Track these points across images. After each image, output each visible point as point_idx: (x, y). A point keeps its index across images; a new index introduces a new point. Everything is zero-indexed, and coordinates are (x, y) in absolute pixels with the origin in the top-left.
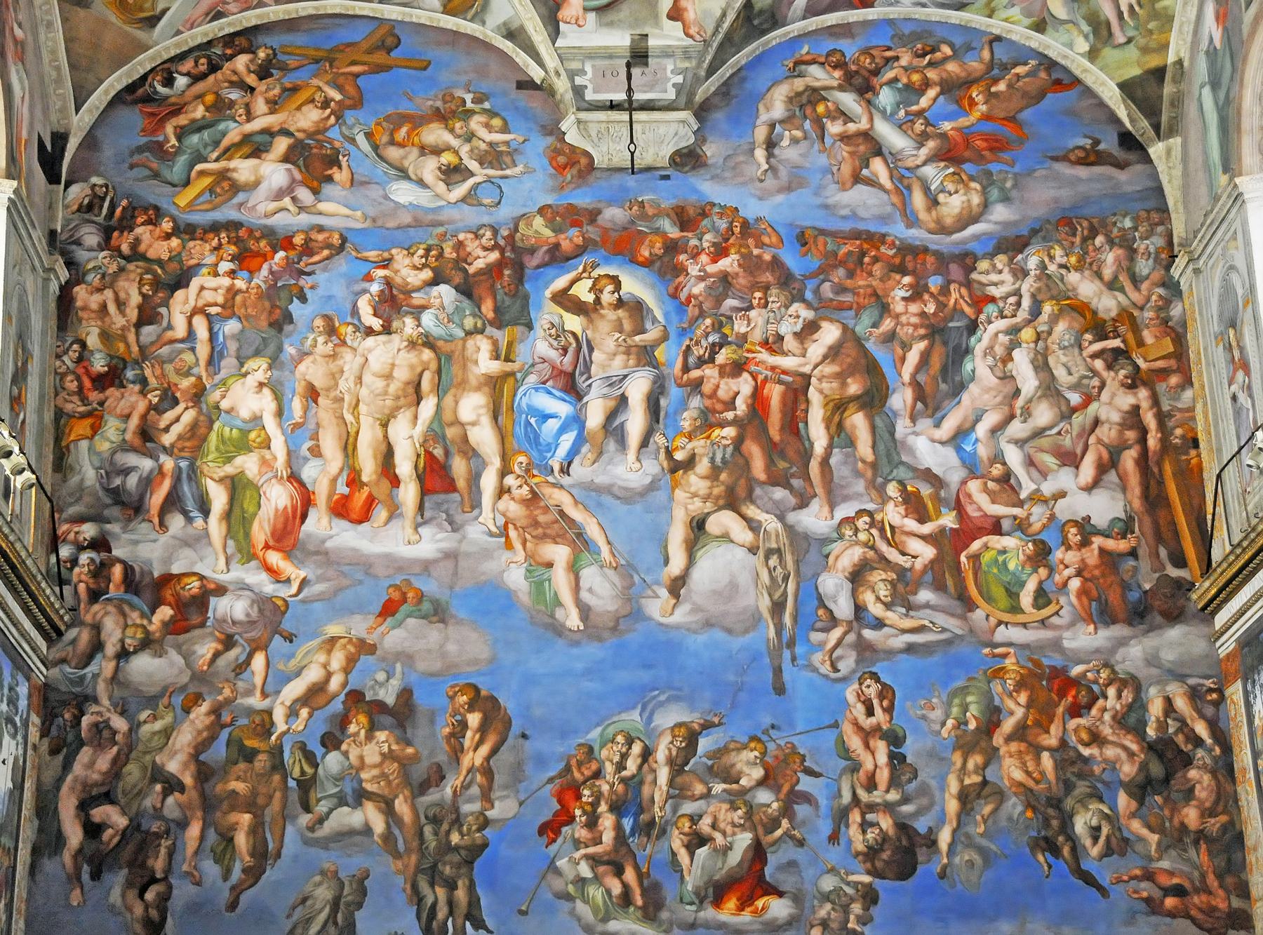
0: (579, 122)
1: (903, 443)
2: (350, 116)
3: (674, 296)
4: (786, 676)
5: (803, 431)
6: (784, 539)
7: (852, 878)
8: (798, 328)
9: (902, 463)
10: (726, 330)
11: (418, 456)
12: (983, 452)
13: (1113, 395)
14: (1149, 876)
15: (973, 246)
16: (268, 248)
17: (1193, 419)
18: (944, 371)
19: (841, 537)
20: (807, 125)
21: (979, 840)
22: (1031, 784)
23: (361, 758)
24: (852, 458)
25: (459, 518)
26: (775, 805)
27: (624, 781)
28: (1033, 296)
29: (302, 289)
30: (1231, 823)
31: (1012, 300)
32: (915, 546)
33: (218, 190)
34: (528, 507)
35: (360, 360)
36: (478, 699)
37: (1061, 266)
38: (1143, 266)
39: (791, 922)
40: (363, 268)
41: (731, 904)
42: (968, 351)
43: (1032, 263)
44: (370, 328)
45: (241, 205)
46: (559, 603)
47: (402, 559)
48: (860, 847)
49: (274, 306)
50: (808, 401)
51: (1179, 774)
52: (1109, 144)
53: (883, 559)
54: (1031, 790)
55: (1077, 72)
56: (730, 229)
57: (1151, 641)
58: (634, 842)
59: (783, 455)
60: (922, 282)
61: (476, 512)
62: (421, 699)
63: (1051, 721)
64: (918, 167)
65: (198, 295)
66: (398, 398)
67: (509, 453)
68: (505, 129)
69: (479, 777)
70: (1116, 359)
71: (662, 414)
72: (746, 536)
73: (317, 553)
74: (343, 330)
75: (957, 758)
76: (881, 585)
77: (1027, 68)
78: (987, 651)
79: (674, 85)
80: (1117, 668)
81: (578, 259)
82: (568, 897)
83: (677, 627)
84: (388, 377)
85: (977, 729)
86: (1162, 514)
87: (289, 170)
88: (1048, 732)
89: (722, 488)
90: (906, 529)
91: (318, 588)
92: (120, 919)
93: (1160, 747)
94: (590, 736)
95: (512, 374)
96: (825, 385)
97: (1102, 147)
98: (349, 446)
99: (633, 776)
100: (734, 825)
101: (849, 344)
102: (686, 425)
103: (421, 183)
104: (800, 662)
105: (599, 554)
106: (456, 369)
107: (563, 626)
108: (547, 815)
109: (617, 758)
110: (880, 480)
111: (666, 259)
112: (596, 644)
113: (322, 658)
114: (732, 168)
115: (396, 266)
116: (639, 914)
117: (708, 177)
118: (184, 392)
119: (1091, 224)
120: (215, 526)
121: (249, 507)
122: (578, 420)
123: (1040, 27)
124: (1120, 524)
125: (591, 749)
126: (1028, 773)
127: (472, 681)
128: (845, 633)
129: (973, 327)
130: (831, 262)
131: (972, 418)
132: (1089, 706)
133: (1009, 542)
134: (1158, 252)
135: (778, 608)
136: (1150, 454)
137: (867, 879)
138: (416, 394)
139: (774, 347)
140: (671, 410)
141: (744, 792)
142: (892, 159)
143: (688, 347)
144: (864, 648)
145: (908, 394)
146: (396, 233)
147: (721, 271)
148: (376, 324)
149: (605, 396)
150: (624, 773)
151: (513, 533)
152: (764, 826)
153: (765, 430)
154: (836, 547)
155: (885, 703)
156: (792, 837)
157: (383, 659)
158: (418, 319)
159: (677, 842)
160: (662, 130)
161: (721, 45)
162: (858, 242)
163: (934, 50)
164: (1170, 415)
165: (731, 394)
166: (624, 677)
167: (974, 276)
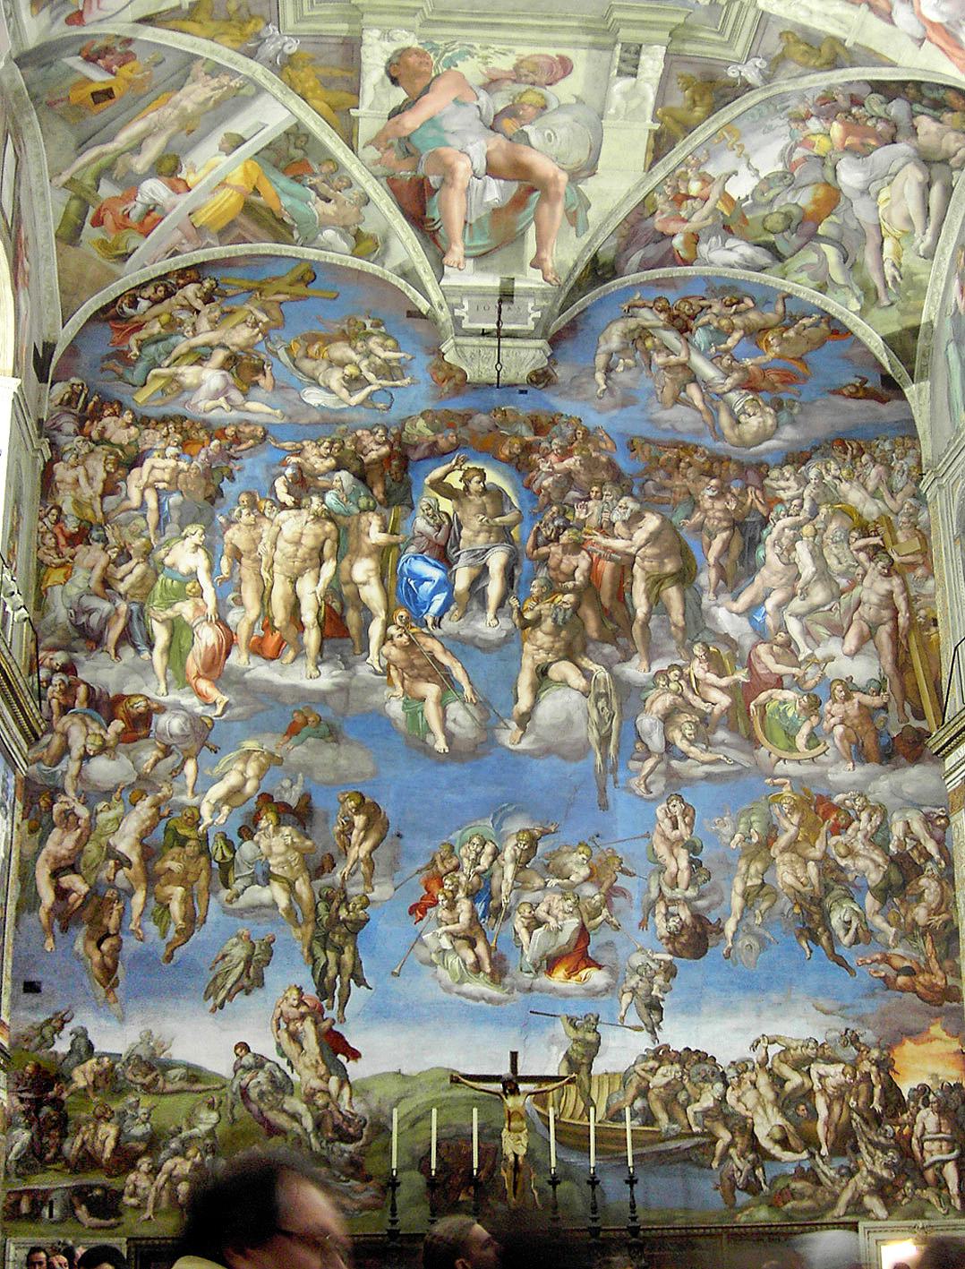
0: (456, 345)
2: (274, 335)
3: (528, 488)
5: (628, 600)
6: (611, 686)
8: (626, 517)
12: (770, 621)
15: (769, 459)
18: (742, 556)
19: (656, 686)
20: (638, 355)
21: (756, 929)
22: (799, 887)
23: (270, 848)
25: (351, 660)
26: (597, 897)
27: (477, 873)
28: (813, 499)
30: (951, 920)
31: (796, 502)
32: (715, 695)
34: (406, 651)
38: (898, 481)
39: (608, 989)
41: (560, 973)
43: (813, 474)
46: (431, 732)
47: (304, 689)
48: (664, 932)
49: (208, 484)
50: (632, 576)
52: (874, 383)
55: (850, 326)
61: (364, 655)
62: (319, 803)
66: (304, 561)
67: (393, 608)
68: (397, 349)
72: (581, 683)
73: (237, 683)
75: (742, 865)
76: (687, 725)
78: (768, 781)
82: (432, 964)
84: (298, 543)
86: (907, 677)
91: (238, 710)
95: (397, 545)
98: (265, 598)
102: (535, 591)
103: (328, 389)
104: (620, 785)
105: (462, 691)
106: (352, 539)
107: (433, 748)
109: (472, 856)
113: (240, 766)
114: (575, 388)
115: (307, 455)
116: (488, 978)
118: (137, 550)
120: (158, 659)
121: (187, 646)
122: (447, 584)
123: (822, 289)
125: (452, 848)
128: (657, 763)
129: (765, 522)
131: (762, 594)
133: (789, 695)
135: (604, 740)
137: (669, 957)
140: (523, 579)
141: (573, 886)
142: (705, 386)
144: (671, 774)
145: (713, 574)
148: (289, 500)
149: (470, 565)
150: (478, 868)
151: (393, 673)
153: (598, 597)
154: (653, 694)
155: (687, 819)
157: (287, 770)
159: (519, 923)
160: (523, 354)
166: (480, 792)
167: (767, 482)
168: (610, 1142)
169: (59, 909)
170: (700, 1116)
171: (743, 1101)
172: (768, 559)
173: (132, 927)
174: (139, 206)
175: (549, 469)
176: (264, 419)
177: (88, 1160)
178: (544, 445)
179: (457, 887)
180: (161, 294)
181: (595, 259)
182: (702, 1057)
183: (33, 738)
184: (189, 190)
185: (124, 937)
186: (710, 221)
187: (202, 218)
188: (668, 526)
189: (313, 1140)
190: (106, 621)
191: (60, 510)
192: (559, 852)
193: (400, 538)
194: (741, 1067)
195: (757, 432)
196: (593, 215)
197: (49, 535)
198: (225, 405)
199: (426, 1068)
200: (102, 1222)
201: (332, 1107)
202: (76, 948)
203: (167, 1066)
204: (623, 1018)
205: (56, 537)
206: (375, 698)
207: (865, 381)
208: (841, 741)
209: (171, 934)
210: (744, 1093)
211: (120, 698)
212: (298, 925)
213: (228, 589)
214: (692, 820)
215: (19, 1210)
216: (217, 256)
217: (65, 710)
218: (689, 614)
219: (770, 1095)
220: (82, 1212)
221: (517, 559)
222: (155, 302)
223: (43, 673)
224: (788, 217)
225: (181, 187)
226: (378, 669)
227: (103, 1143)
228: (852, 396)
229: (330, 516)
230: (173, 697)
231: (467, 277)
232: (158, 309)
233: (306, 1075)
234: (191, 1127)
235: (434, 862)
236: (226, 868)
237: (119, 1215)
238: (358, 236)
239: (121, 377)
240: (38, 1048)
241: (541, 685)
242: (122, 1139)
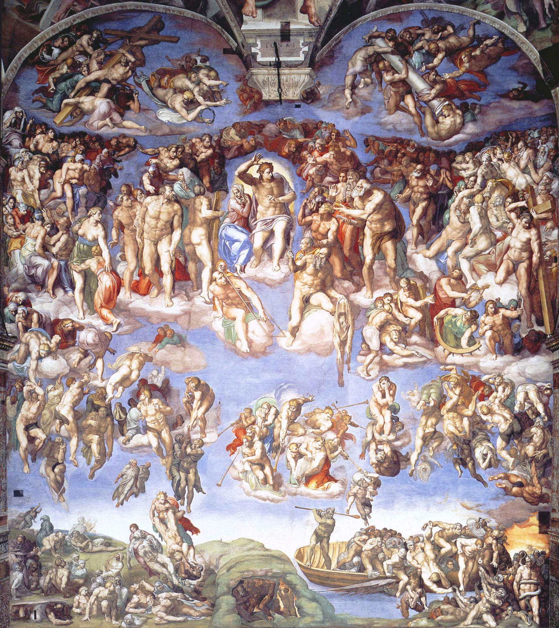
1: (410, 258)
2: (138, 70)
3: (300, 175)
4: (345, 378)
5: (360, 251)
6: (348, 308)
7: (369, 475)
8: (362, 193)
9: (409, 268)
10: (325, 195)
11: (172, 261)
12: (450, 263)
13: (519, 232)
14: (507, 477)
15: (456, 148)
16: (99, 147)
19: (376, 307)
20: (373, 75)
21: (429, 458)
22: (457, 432)
23: (146, 411)
24: (384, 265)
25: (191, 294)
26: (336, 440)
27: (266, 426)
28: (483, 176)
29: (115, 170)
31: (472, 179)
33: (75, 114)
34: (224, 289)
37: (500, 159)
38: (541, 160)
40: (146, 158)
41: (313, 484)
43: (484, 158)
44: (149, 191)
45: (86, 123)
48: (375, 461)
50: (364, 234)
51: (527, 430)
53: (396, 319)
55: (519, 44)
56: (330, 137)
58: (270, 455)
59: (350, 264)
60: (427, 168)
61: (199, 291)
62: (175, 385)
63: (470, 402)
64: (430, 100)
65: (67, 173)
66: (162, 230)
68: (217, 78)
69: (200, 423)
70: (522, 213)
71: (291, 240)
74: (135, 193)
75: (423, 420)
76: (394, 332)
77: (492, 41)
78: (442, 367)
79: (304, 52)
80: (504, 377)
81: (252, 154)
83: (295, 351)
85: (434, 406)
87: (108, 102)
88: (468, 408)
89: (319, 280)
90: (409, 304)
91: (126, 328)
92: (45, 480)
93: (520, 416)
94: (251, 404)
95: (218, 218)
96: (373, 226)
97: (527, 89)
98: (139, 256)
99: (271, 424)
101: (386, 203)
102: (303, 246)
103: (174, 110)
104: (351, 371)
106: (190, 215)
108: (231, 442)
109: (263, 415)
110: (397, 277)
111: (297, 154)
112: (254, 360)
113: (128, 362)
114: (333, 100)
115: (162, 157)
116: (271, 488)
117: (320, 106)
118: (61, 225)
119: (517, 135)
121: (94, 287)
122: (249, 243)
124: (515, 303)
125: (251, 411)
126: (456, 427)
128: (374, 357)
129: (450, 194)
132: (489, 396)
133: (458, 311)
135: (343, 343)
136: (533, 265)
137: (376, 475)
139: (349, 204)
140: (295, 239)
142: (417, 96)
143: (306, 203)
145: (415, 231)
146: (161, 138)
147: (324, 161)
148: (151, 189)
149: (263, 230)
151: (217, 302)
152: (330, 450)
153: (342, 249)
154: (373, 313)
155: (391, 392)
158: (172, 187)
159: (289, 455)
162: (395, 145)
163: (445, 29)
165: (326, 230)
166: (268, 376)
167: (454, 165)
169: (31, 447)
170: (390, 567)
172: (451, 219)
173: (71, 458)
177: (53, 589)
178: (311, 144)
179: (254, 434)
180: (66, 43)
182: (393, 534)
185: (66, 464)
188: (388, 199)
189: (174, 578)
192: (314, 413)
194: (416, 540)
195: (450, 128)
197: (10, 217)
198: (110, 124)
200: (63, 621)
201: (184, 559)
202: (41, 471)
203: (93, 537)
204: (348, 511)
205: (14, 218)
206: (206, 319)
208: (490, 340)
209: (93, 462)
211: (57, 321)
212: (163, 457)
214: (394, 392)
215: (19, 616)
217: (26, 329)
218: (399, 260)
219: (432, 556)
220: (51, 616)
221: (292, 225)
222: (63, 49)
223: (12, 306)
226: (208, 300)
227: (61, 579)
228: (516, 98)
229: (176, 199)
232: (65, 55)
236: (122, 423)
237: (70, 618)
239: (45, 106)
240: (24, 527)
242: (71, 577)
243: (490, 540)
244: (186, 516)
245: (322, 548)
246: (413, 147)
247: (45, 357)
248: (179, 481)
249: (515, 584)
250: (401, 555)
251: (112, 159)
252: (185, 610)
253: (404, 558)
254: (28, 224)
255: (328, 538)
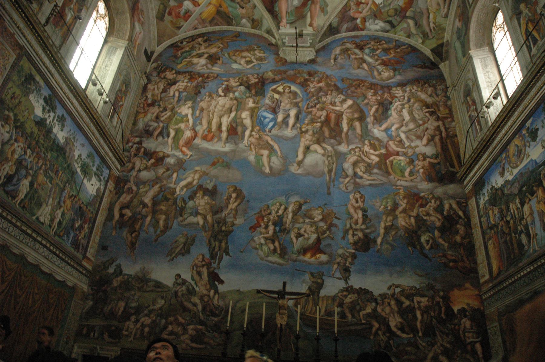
1: (370, 130)
2: (224, 50)
3: (306, 91)
4: (331, 190)
6: (333, 153)
7: (348, 250)
8: (341, 100)
12: (394, 134)
14: (445, 256)
15: (392, 85)
17: (455, 130)
18: (383, 112)
19: (351, 153)
20: (346, 55)
21: (390, 241)
22: (408, 226)
23: (199, 203)
26: (325, 227)
27: (278, 216)
28: (408, 97)
31: (402, 97)
32: (373, 157)
35: (216, 102)
36: (235, 190)
38: (439, 92)
39: (327, 262)
41: (308, 255)
42: (389, 109)
43: (408, 89)
46: (263, 165)
48: (351, 241)
50: (342, 118)
53: (363, 160)
54: (407, 228)
55: (419, 48)
56: (323, 77)
57: (445, 188)
59: (334, 131)
62: (219, 188)
63: (414, 207)
66: (225, 112)
68: (264, 53)
69: (233, 212)
72: (322, 151)
75: (384, 217)
78: (394, 187)
82: (256, 249)
85: (391, 209)
88: (413, 211)
91: (194, 157)
95: (258, 107)
96: (348, 115)
98: (210, 122)
100: (311, 232)
102: (306, 121)
103: (240, 64)
104: (336, 186)
105: (277, 153)
107: (264, 172)
109: (276, 210)
113: (192, 175)
116: (278, 255)
120: (170, 140)
122: (275, 119)
123: (409, 36)
125: (268, 206)
126: (406, 223)
127: (236, 185)
128: (350, 180)
129: (391, 103)
130: (351, 85)
133: (402, 158)
134: (443, 90)
135: (330, 171)
137: (353, 251)
138: (230, 110)
141: (315, 223)
142: (369, 64)
144: (356, 184)
145: (372, 118)
148: (222, 94)
149: (283, 114)
150: (278, 214)
151: (252, 147)
154: (349, 156)
156: (330, 237)
159: (293, 235)
160: (306, 52)
161: (323, 36)
163: (380, 42)
164: (448, 128)
167: (391, 91)
168: (327, 325)
171: (384, 311)
173: (145, 229)
174: (183, 11)
175: (313, 87)
176: (217, 72)
178: (312, 79)
181: (330, 25)
182: (367, 292)
183: (122, 163)
184: (199, 5)
186: (369, 13)
187: (204, 16)
189: (201, 315)
190: (155, 129)
191: (147, 97)
192: (311, 210)
193: (259, 105)
194: (383, 296)
196: (329, 9)
199: (251, 289)
200: (113, 341)
201: (210, 302)
204: (333, 274)
205: (144, 105)
206: (245, 154)
207: (425, 63)
210: (385, 308)
211: (155, 152)
212: (206, 231)
213: (197, 120)
216: (210, 31)
217: (135, 155)
219: (396, 309)
220: (106, 336)
222: (188, 42)
223: (130, 144)
224: (396, 10)
225: (197, 4)
227: (119, 309)
230: (173, 152)
231: (287, 30)
232: (188, 44)
233: (201, 289)
234: (153, 305)
235: (261, 211)
236: (183, 209)
238: (253, 21)
239: (174, 61)
241: (307, 151)
243: (438, 299)
244: (216, 271)
245: (314, 300)
246: (368, 83)
247: (143, 170)
248: (215, 247)
249: (461, 332)
250: (373, 307)
251: (204, 82)
252: (206, 340)
253: (375, 310)
254: (151, 108)
255: (319, 292)
